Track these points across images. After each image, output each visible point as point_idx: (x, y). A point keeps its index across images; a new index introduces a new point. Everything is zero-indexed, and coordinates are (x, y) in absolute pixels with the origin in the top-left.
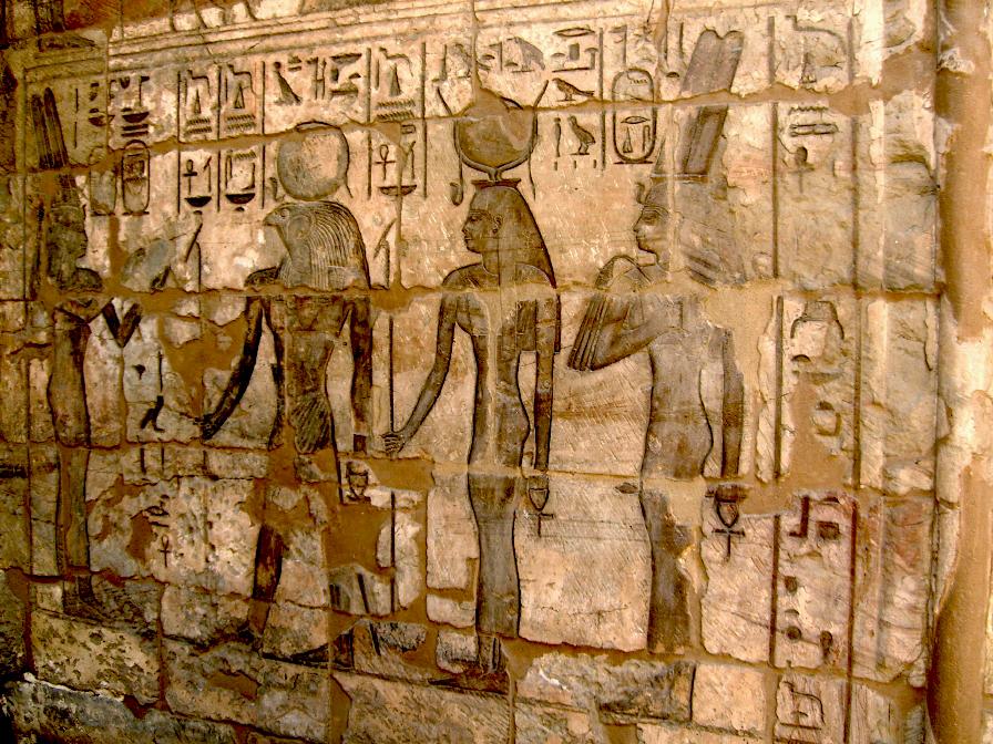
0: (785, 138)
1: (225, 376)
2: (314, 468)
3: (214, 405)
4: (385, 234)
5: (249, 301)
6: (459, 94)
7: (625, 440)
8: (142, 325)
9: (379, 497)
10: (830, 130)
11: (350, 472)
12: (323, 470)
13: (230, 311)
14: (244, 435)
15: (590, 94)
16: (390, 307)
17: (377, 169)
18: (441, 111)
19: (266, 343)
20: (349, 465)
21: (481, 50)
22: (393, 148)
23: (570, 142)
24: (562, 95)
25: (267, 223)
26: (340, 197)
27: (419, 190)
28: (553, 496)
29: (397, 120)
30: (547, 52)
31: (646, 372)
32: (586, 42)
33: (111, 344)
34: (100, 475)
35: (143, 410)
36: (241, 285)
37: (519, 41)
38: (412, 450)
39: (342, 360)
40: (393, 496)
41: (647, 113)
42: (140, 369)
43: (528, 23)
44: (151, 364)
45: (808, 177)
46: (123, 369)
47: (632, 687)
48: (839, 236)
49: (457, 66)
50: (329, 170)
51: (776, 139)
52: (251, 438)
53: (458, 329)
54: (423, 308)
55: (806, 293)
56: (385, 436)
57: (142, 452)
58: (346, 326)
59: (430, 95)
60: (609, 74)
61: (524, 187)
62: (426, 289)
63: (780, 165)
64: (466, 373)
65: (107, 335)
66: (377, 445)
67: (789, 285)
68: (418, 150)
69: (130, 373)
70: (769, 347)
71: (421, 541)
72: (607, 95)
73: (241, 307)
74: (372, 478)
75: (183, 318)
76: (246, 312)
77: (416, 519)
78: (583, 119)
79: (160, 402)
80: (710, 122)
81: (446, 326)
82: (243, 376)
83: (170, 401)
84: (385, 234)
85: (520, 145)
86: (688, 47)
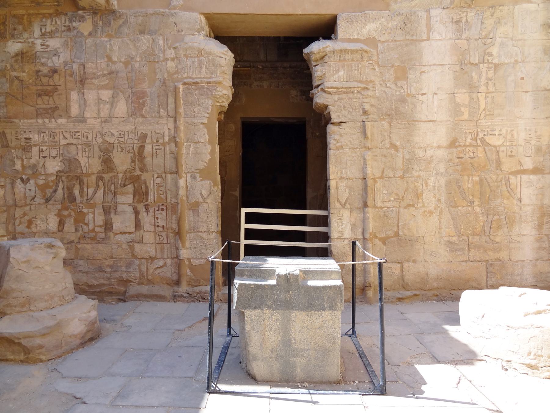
0: (154, 150)
1: (51, 190)
2: (72, 206)
3: (48, 196)
4: (86, 164)
5: (57, 176)
6: (100, 140)
7: (129, 199)
8: (30, 181)
9: (85, 211)
10: (161, 149)
11: (79, 207)
12: (73, 207)
13: (53, 178)
14: (56, 201)
15: (123, 142)
16: (87, 177)
17: (84, 153)
18: (96, 143)
19: (61, 183)
20: (79, 205)
21: (103, 133)
22: (87, 149)
23: (119, 150)
24: (118, 142)
25: (61, 161)
26: (77, 157)
27: (92, 157)
28: (118, 208)
29: (88, 144)
30: (115, 134)
31: (133, 187)
32: (122, 133)
33: (22, 185)
34: (18, 213)
35: (31, 198)
36: (55, 173)
37: (110, 132)
38: (92, 202)
39: (77, 186)
40: (88, 210)
41: (132, 145)
42: (30, 190)
43: (112, 129)
44: (33, 189)
45: (158, 156)
46: (25, 190)
47: (132, 239)
48: (162, 165)
49: (99, 136)
50: (75, 152)
51: (153, 150)
52: (57, 202)
53: (100, 180)
54: (93, 177)
55: (158, 173)
56: (86, 200)
57: (30, 207)
58: (78, 180)
59: (94, 140)
60: (126, 139)
61: (112, 157)
62: (93, 174)
63: (153, 154)
64: (102, 188)
65: (21, 183)
66: (85, 201)
67: (155, 173)
68: (92, 150)
69: (27, 190)
70: (152, 182)
71: (94, 218)
72: (126, 142)
73: (55, 177)
74: (84, 207)
75: (41, 179)
76: (56, 178)
77: (93, 214)
78: (122, 146)
79: (35, 196)
80: (142, 147)
81: (98, 180)
82: (55, 191)
83: (38, 196)
84: (86, 164)
85: (111, 149)
86: (139, 135)
